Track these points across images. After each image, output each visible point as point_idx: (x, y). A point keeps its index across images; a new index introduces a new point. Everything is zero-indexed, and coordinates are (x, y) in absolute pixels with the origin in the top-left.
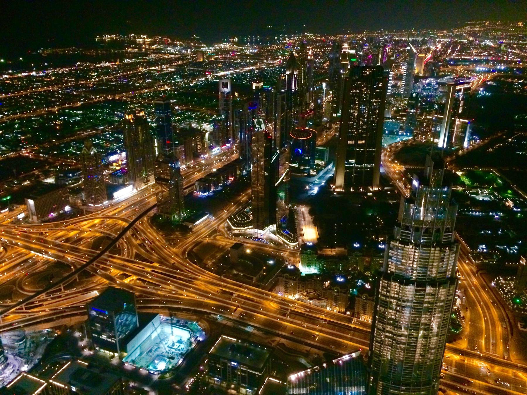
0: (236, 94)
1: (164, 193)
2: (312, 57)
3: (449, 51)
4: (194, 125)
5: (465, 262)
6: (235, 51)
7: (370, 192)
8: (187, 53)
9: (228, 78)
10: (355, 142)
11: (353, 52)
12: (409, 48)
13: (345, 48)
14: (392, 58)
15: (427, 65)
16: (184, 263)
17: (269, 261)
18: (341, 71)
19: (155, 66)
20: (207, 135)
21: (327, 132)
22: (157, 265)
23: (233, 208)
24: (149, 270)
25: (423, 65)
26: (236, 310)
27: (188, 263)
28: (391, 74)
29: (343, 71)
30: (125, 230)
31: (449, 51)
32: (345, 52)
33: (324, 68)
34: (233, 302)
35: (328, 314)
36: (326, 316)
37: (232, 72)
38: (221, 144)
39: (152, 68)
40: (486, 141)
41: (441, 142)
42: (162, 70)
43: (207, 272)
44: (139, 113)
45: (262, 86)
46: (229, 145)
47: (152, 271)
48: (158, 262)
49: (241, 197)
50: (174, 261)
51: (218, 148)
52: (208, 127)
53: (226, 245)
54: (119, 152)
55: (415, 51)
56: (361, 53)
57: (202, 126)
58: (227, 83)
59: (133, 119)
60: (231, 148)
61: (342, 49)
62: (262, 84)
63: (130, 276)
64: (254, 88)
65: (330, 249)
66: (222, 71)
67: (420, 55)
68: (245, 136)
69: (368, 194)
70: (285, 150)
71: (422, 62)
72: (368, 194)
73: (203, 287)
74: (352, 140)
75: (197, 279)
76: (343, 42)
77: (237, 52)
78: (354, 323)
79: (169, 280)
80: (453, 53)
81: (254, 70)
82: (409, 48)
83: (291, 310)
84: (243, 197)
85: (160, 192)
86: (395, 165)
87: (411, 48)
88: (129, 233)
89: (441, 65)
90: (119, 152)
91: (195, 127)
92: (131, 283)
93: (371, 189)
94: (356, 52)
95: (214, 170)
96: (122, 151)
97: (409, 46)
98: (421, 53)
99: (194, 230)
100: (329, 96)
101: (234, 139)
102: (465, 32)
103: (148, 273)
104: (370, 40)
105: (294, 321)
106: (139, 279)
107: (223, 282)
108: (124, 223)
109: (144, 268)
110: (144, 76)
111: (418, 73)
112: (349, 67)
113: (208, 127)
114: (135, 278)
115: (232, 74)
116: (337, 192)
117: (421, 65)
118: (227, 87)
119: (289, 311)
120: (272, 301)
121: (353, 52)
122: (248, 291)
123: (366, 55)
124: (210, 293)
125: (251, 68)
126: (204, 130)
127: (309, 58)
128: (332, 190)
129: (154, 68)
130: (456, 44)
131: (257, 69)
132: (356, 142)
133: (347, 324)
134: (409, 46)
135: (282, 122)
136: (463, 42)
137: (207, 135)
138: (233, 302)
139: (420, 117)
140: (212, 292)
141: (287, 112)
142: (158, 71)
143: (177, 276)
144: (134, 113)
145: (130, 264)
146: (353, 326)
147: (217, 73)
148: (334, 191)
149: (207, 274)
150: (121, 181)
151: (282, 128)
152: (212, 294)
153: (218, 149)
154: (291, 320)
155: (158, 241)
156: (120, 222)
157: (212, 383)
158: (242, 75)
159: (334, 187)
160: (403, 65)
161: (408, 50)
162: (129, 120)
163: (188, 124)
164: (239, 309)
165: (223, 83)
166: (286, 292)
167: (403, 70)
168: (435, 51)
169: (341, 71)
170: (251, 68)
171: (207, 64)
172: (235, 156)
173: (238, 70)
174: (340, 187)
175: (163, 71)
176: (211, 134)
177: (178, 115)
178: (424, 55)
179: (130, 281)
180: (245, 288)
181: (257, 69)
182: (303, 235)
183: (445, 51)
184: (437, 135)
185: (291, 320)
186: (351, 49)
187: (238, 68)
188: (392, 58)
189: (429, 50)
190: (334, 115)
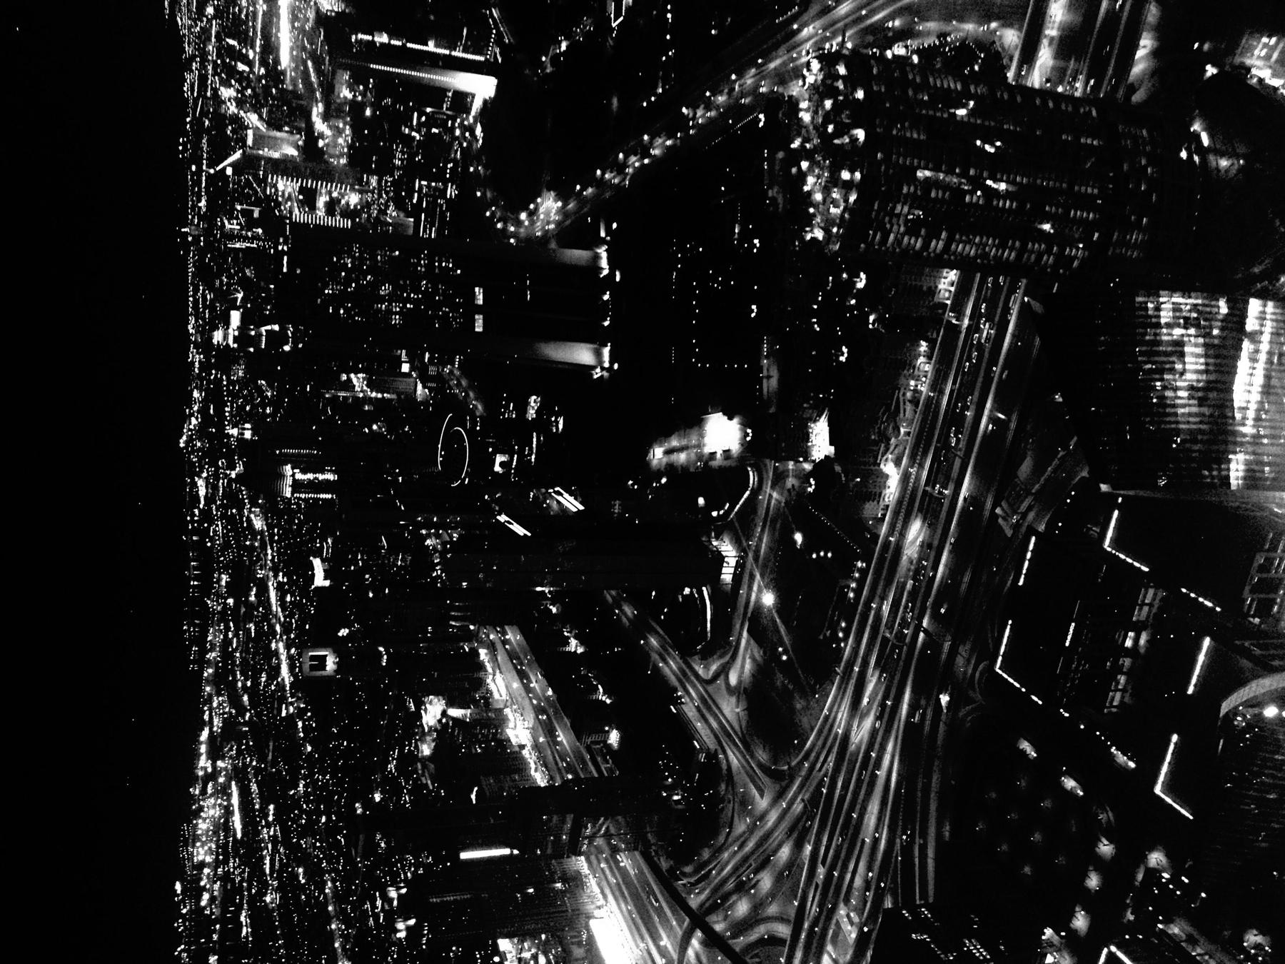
0: (344, 632)
1: (613, 830)
2: (248, 426)
3: (241, 67)
4: (426, 750)
5: (799, 30)
6: (226, 635)
7: (612, 274)
8: (226, 769)
9: (300, 655)
10: (479, 313)
11: (235, 317)
12: (229, 171)
13: (225, 337)
14: (256, 215)
15: (273, 124)
16: (803, 773)
17: (795, 542)
18: (287, 348)
19: (263, 858)
20: (455, 713)
21: (451, 388)
22: (808, 848)
23: (654, 642)
24: (821, 871)
25: (278, 134)
26: (925, 631)
27: (801, 763)
28: (298, 215)
29: (287, 344)
30: (713, 940)
31: (241, 67)
32: (236, 339)
34: (908, 640)
35: (937, 385)
36: (941, 392)
37: (281, 645)
38: (482, 674)
39: (268, 871)
41: (482, 87)
42: (274, 839)
43: (826, 711)
44: (391, 901)
45: (323, 561)
46: (483, 654)
47: (823, 863)
48: (798, 846)
49: (624, 620)
50: (799, 799)
51: (489, 681)
52: (433, 711)
53: (753, 659)
54: (497, 959)
55: (237, 155)
56: (240, 296)
57: (430, 728)
58: (313, 658)
59: (406, 919)
60: (492, 647)
61: (228, 345)
62: (317, 563)
63: (838, 925)
64: (327, 583)
65: (765, 381)
66: (277, 669)
67: (250, 142)
68: (458, 609)
69: (618, 279)
70: (497, 501)
71: (269, 137)
72: (618, 279)
73: (868, 723)
74: (474, 321)
75: (846, 737)
76: (206, 345)
77: (227, 629)
78: (960, 317)
79: (849, 817)
80: (246, 56)
81: (279, 583)
82: (229, 171)
83: (925, 485)
84: (625, 614)
85: (609, 844)
86: (542, 210)
87: (229, 165)
88: (719, 927)
89: (277, 88)
90: (497, 959)
91: (433, 744)
92: (856, 919)
93: (605, 272)
94: (237, 308)
95: (550, 692)
96: (496, 951)
97: (224, 169)
98: (244, 140)
99: (711, 743)
100: (355, 381)
101: (471, 636)
102: (190, 27)
103: (829, 876)
104: (206, 275)
105: (955, 473)
106: (847, 901)
107: (852, 670)
108: (695, 943)
109: (817, 885)
110: (288, 886)
111: (297, 147)
112: (276, 328)
113: (433, 711)
114: (842, 911)
115: (288, 647)
116: (612, 363)
117: (276, 138)
118: (323, 659)
119: (927, 488)
120: (902, 535)
121: (235, 317)
122: (877, 599)
123: (245, 283)
124: (883, 705)
125: (273, 595)
126: (440, 721)
127: (248, 435)
128: (606, 374)
129: (267, 861)
130: (224, 51)
131: (276, 576)
132: (479, 310)
133: (963, 336)
134: (224, 169)
137: (455, 713)
138: (908, 640)
140: (879, 697)
141: (396, 496)
142: (275, 850)
143: (838, 791)
144: (391, 916)
145: (806, 925)
146: (966, 322)
147: (284, 686)
148: (610, 369)
149: (830, 710)
150: (578, 952)
152: (885, 697)
153: (494, 680)
154: (951, 486)
155: (741, 847)
156: (690, 953)
157: (1123, 697)
158: (291, 616)
159: (598, 370)
160: (275, 186)
161: (234, 174)
162: (408, 929)
163: (424, 767)
164: (925, 623)
165: (312, 668)
166: (877, 496)
167: (286, 186)
168: (240, 103)
169: (287, 348)
170: (273, 595)
171: (259, 715)
172: (513, 636)
173: (278, 628)
174: (598, 354)
175: (275, 836)
176: (451, 704)
177: (398, 792)
178: (250, 132)
179: (852, 923)
180: (867, 607)
181: (276, 576)
182: (727, 453)
183: (241, 78)
184: (462, 100)
185: (951, 486)
186: (227, 323)
187: (272, 627)
188: (256, 215)
189: (236, 120)
190: (405, 368)
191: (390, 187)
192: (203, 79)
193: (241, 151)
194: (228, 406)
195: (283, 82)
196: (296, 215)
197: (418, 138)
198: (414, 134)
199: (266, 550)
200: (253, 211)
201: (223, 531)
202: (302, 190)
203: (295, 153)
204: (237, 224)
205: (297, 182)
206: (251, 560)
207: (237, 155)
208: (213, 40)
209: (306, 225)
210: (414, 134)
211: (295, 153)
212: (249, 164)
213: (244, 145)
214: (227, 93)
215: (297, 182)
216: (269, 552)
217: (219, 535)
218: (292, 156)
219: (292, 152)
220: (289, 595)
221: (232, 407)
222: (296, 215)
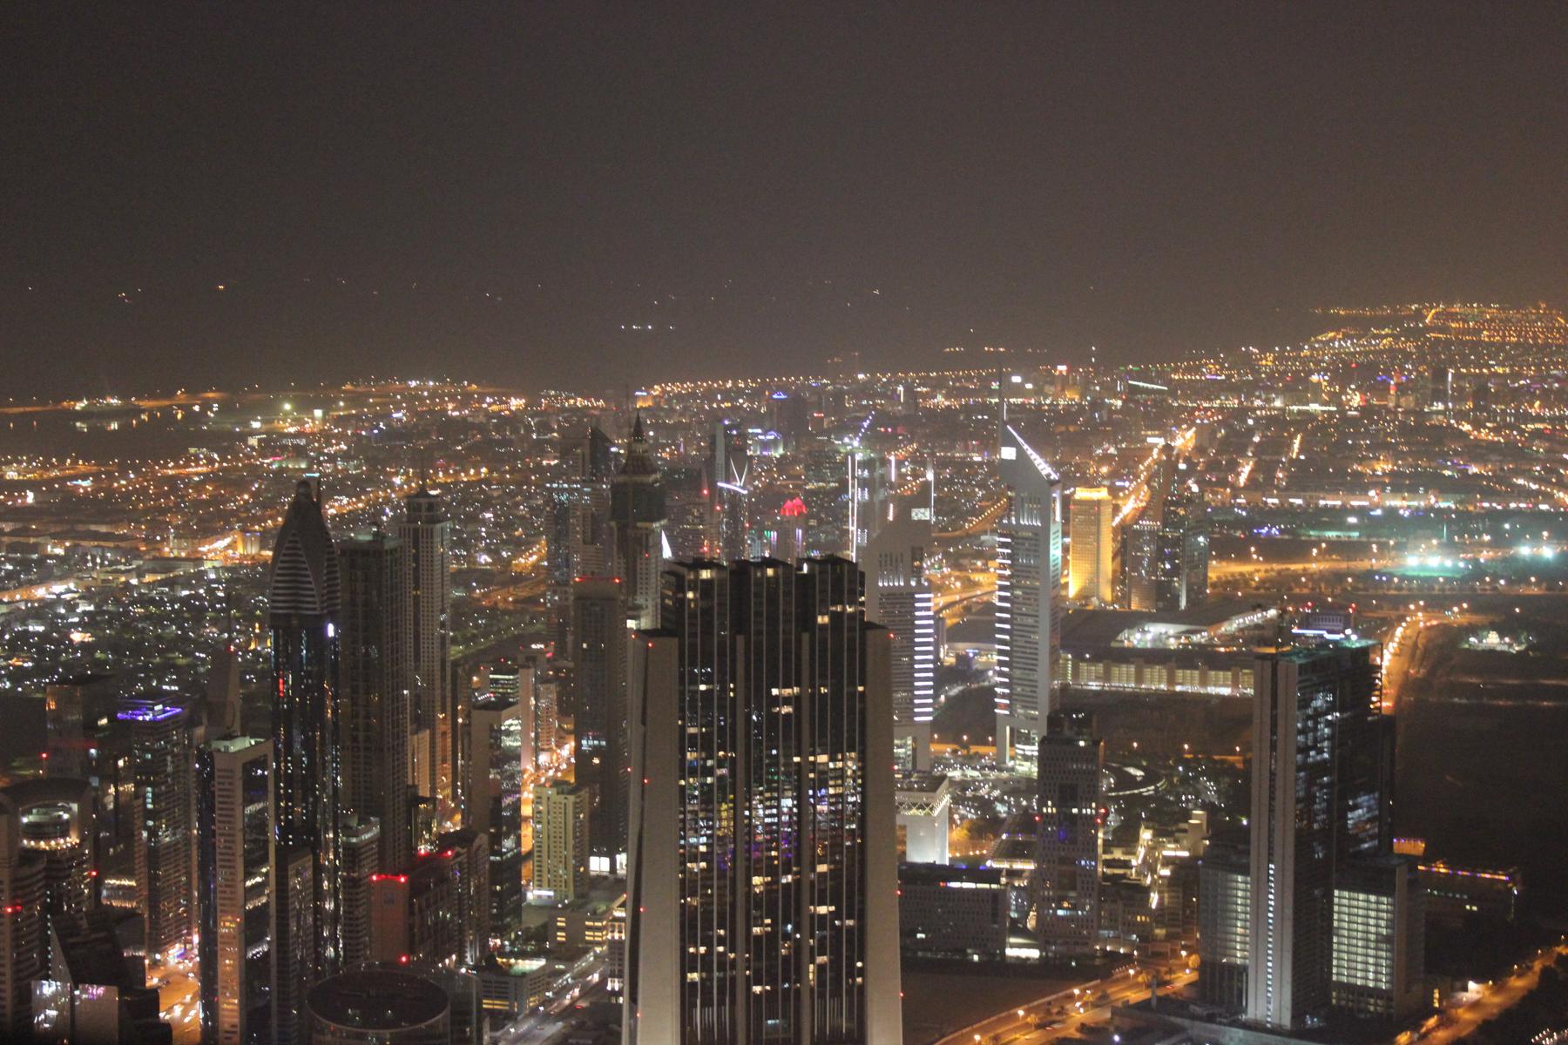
12: (1008, 453)
28: (930, 604)
33: (519, 579)
40: (1518, 983)
55: (1044, 468)
67: (1082, 494)
71: (1098, 532)
82: (1008, 453)
87: (1020, 452)
97: (1012, 442)
111: (1085, 595)
135: (253, 926)
136: (1311, 416)
139: (1118, 854)
151: (253, 971)
178: (1102, 494)
191: (1018, 804)
192: (1210, 390)
193: (1054, 476)
194: (491, 471)
195: (1223, 556)
196: (929, 600)
197: (1134, 863)
198: (1141, 851)
199: (154, 571)
200: (926, 505)
201: (198, 474)
202: (989, 608)
203: (1072, 592)
204: (901, 476)
205: (1002, 599)
206: (123, 538)
207: (1044, 468)
208: (1295, 408)
209: (907, 627)
210: (1141, 851)
211: (1072, 592)
212: (1037, 494)
213: (1067, 480)
214: (1185, 440)
215: (1002, 599)
216: (148, 578)
217: (187, 465)
218: (1066, 586)
219: (1074, 584)
220: (41, 629)
221: (487, 482)
222: (929, 600)
